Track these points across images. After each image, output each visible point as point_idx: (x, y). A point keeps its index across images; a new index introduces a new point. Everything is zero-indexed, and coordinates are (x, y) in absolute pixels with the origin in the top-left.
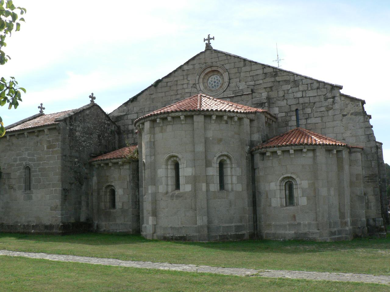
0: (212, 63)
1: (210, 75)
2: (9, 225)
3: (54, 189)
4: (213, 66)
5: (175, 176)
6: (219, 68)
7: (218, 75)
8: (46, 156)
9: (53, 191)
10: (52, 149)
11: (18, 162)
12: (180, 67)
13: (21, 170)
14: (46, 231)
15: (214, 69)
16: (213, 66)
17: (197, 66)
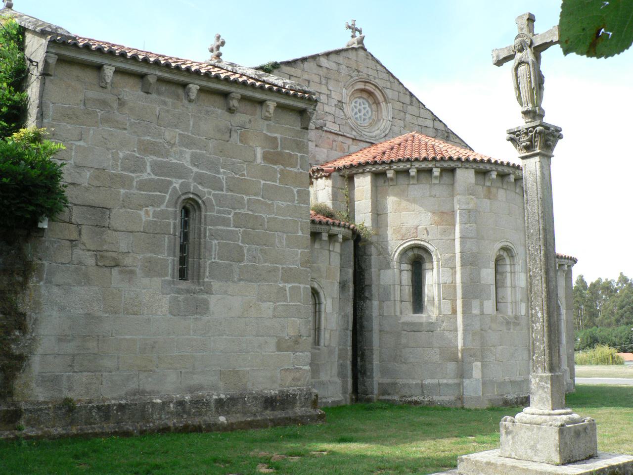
0: (368, 75)
1: (356, 96)
2: (109, 406)
3: (290, 285)
4: (370, 83)
5: (410, 284)
6: (379, 91)
7: (368, 102)
8: (262, 182)
9: (285, 290)
10: (281, 167)
11: (147, 175)
12: (314, 57)
13: (163, 207)
14: (269, 414)
15: (369, 87)
16: (370, 83)
17: (344, 70)
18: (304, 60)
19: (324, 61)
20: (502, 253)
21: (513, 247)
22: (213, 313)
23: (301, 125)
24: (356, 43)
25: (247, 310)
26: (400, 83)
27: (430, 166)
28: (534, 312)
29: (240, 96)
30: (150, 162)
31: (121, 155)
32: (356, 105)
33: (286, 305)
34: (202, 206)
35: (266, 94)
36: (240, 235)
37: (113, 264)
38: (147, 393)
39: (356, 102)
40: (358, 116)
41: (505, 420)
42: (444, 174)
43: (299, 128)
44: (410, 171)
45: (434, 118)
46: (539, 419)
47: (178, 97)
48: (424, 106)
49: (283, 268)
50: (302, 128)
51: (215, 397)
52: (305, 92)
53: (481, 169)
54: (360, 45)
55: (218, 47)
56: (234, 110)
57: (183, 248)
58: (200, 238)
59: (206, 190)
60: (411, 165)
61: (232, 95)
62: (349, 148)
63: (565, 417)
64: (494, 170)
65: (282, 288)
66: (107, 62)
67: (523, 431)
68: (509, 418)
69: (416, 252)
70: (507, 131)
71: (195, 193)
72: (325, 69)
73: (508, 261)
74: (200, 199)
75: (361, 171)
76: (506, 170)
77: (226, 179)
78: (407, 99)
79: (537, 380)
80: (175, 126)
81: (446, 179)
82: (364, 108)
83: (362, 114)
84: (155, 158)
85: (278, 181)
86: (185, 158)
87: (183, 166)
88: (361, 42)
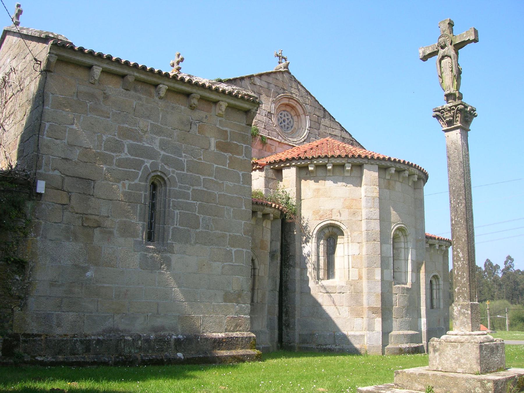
2: (89, 340)
3: (235, 249)
4: (293, 99)
6: (299, 106)
8: (215, 166)
9: (232, 253)
10: (231, 155)
11: (125, 155)
12: (250, 77)
13: (137, 181)
15: (292, 103)
18: (242, 79)
19: (257, 81)
20: (398, 233)
21: (406, 228)
22: (174, 269)
23: (246, 122)
24: (283, 68)
25: (201, 268)
26: (316, 101)
27: (343, 161)
28: (455, 253)
29: (199, 96)
30: (127, 145)
31: (104, 138)
32: (281, 116)
33: (232, 265)
34: (168, 182)
35: (220, 96)
36: (196, 207)
37: (95, 225)
38: (120, 331)
39: (281, 114)
40: (282, 125)
41: (433, 341)
42: (354, 169)
43: (244, 125)
44: (327, 165)
45: (342, 128)
46: (462, 339)
47: (150, 95)
48: (334, 119)
49: (230, 235)
50: (246, 125)
51: (174, 337)
52: (250, 96)
53: (383, 165)
54: (285, 69)
55: (178, 63)
56: (194, 107)
57: (152, 217)
58: (165, 207)
59: (171, 169)
60: (328, 161)
61: (193, 95)
62: (275, 149)
63: (482, 337)
64: (393, 167)
65: (229, 251)
66: (96, 63)
67: (449, 349)
68: (436, 339)
69: (330, 229)
70: (433, 109)
71: (162, 171)
72: (258, 87)
73: (402, 239)
74: (166, 176)
75: (288, 164)
76: (402, 167)
77: (187, 162)
78: (321, 114)
79: (459, 307)
80: (148, 117)
81: (356, 172)
82: (288, 119)
83: (286, 123)
84: (131, 142)
85: (227, 166)
86: (155, 143)
87: (153, 149)
88: (286, 67)
